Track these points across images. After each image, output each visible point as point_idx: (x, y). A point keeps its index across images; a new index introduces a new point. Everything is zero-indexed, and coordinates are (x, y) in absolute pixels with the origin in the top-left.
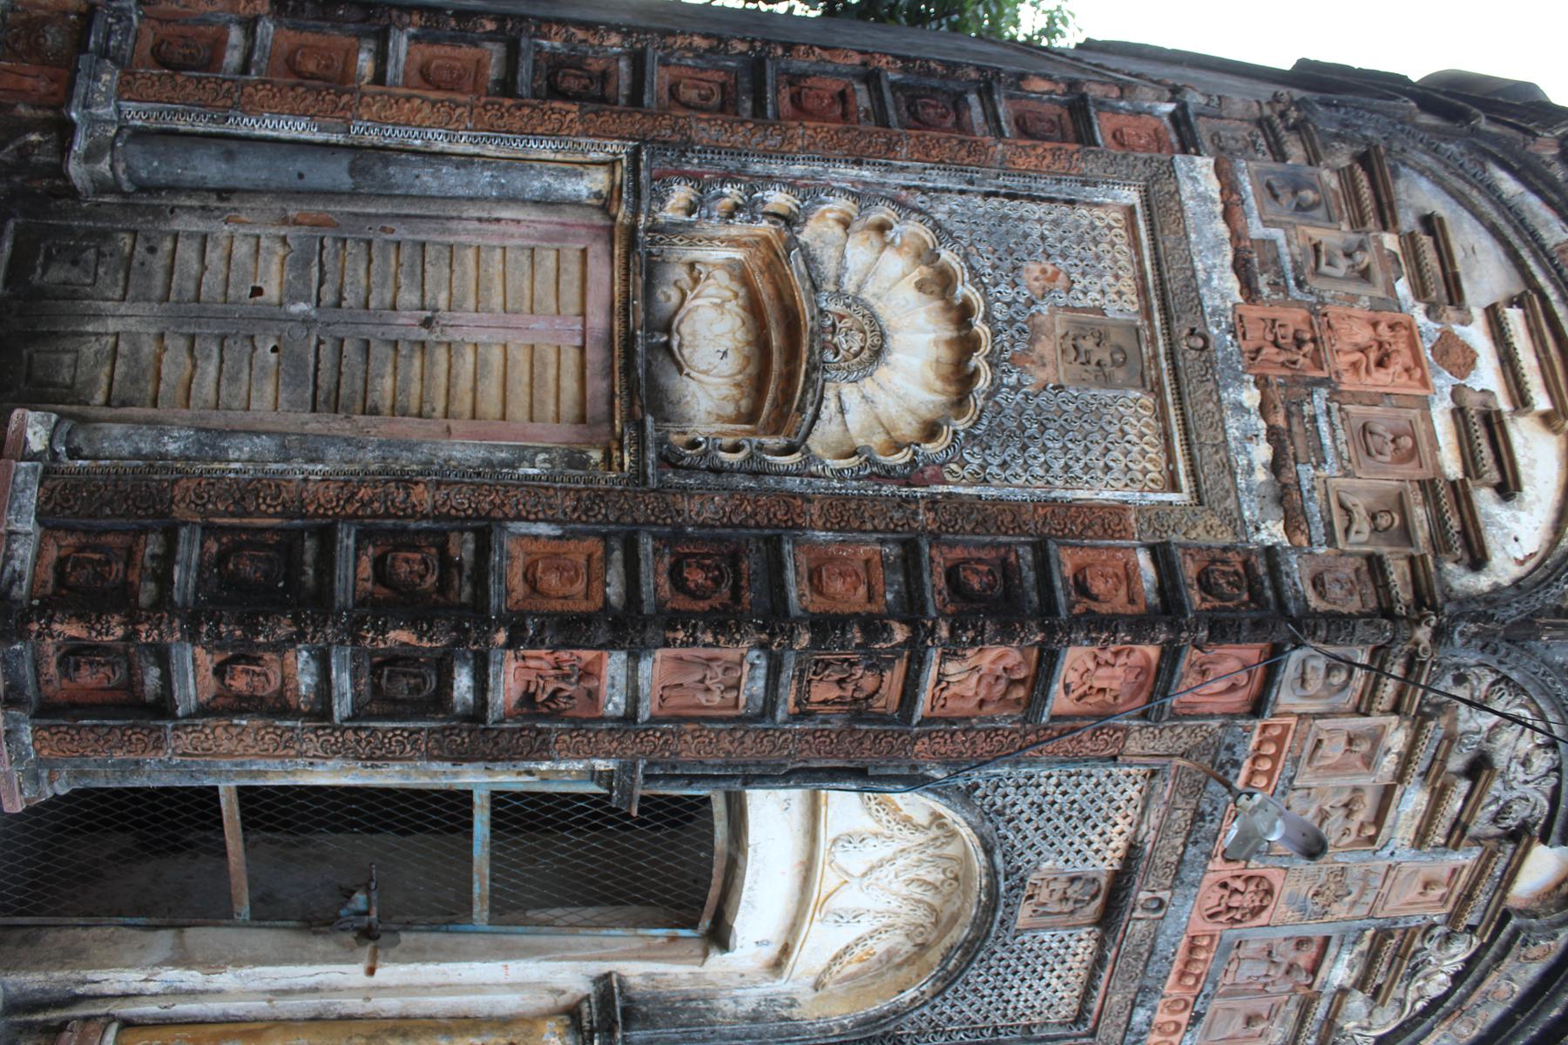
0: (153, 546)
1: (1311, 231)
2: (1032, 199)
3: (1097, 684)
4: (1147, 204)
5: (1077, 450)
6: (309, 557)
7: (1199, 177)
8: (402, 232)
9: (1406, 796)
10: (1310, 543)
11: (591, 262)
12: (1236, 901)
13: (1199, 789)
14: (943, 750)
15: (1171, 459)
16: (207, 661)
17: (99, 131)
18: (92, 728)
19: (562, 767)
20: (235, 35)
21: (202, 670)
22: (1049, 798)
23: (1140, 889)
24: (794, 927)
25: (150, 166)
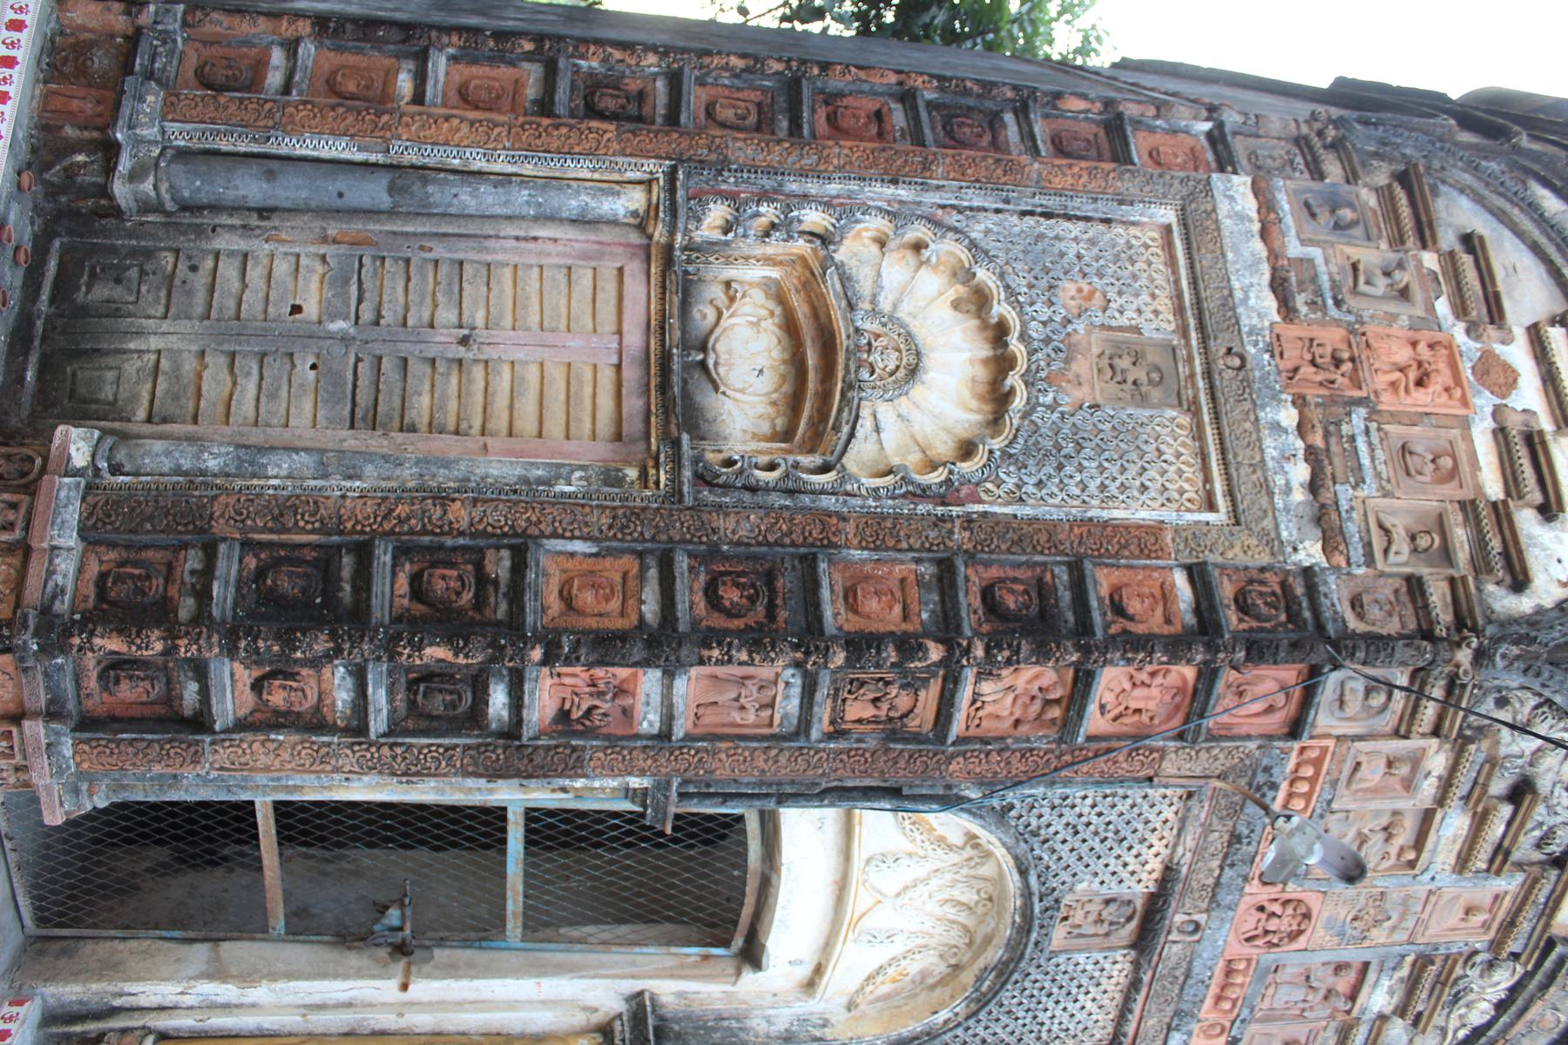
0: (193, 561)
1: (1349, 250)
2: (1068, 218)
3: (1133, 705)
4: (1184, 223)
5: (1114, 469)
6: (346, 573)
7: (1235, 196)
8: (440, 251)
9: (1447, 820)
10: (1349, 563)
11: (627, 280)
12: (1273, 925)
13: (1235, 811)
14: (978, 770)
15: (1207, 479)
16: (245, 676)
17: (143, 151)
18: (131, 742)
19: (597, 784)
20: (277, 57)
21: (240, 685)
22: (1084, 819)
23: (1176, 912)
24: (827, 947)
25: (193, 186)
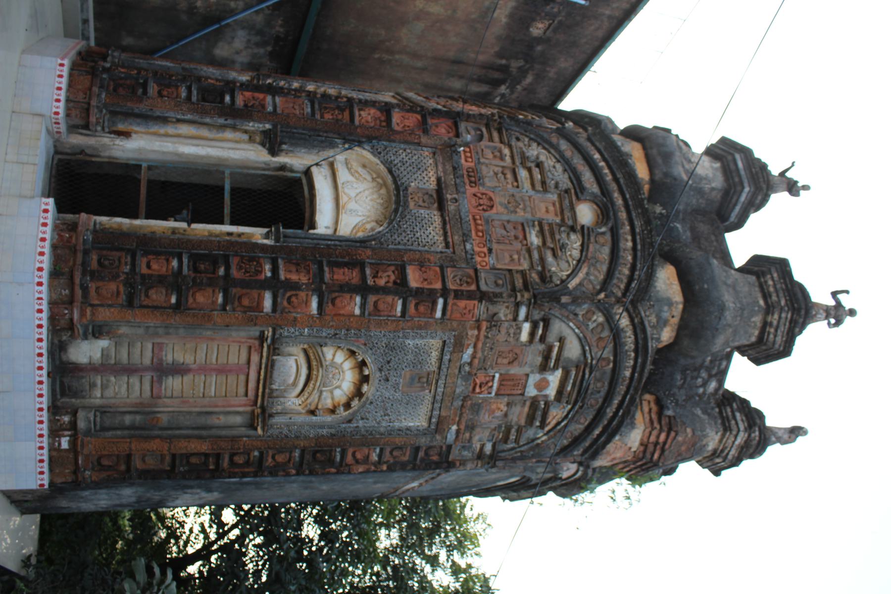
12: (481, 202)
13: (451, 158)
24: (337, 222)
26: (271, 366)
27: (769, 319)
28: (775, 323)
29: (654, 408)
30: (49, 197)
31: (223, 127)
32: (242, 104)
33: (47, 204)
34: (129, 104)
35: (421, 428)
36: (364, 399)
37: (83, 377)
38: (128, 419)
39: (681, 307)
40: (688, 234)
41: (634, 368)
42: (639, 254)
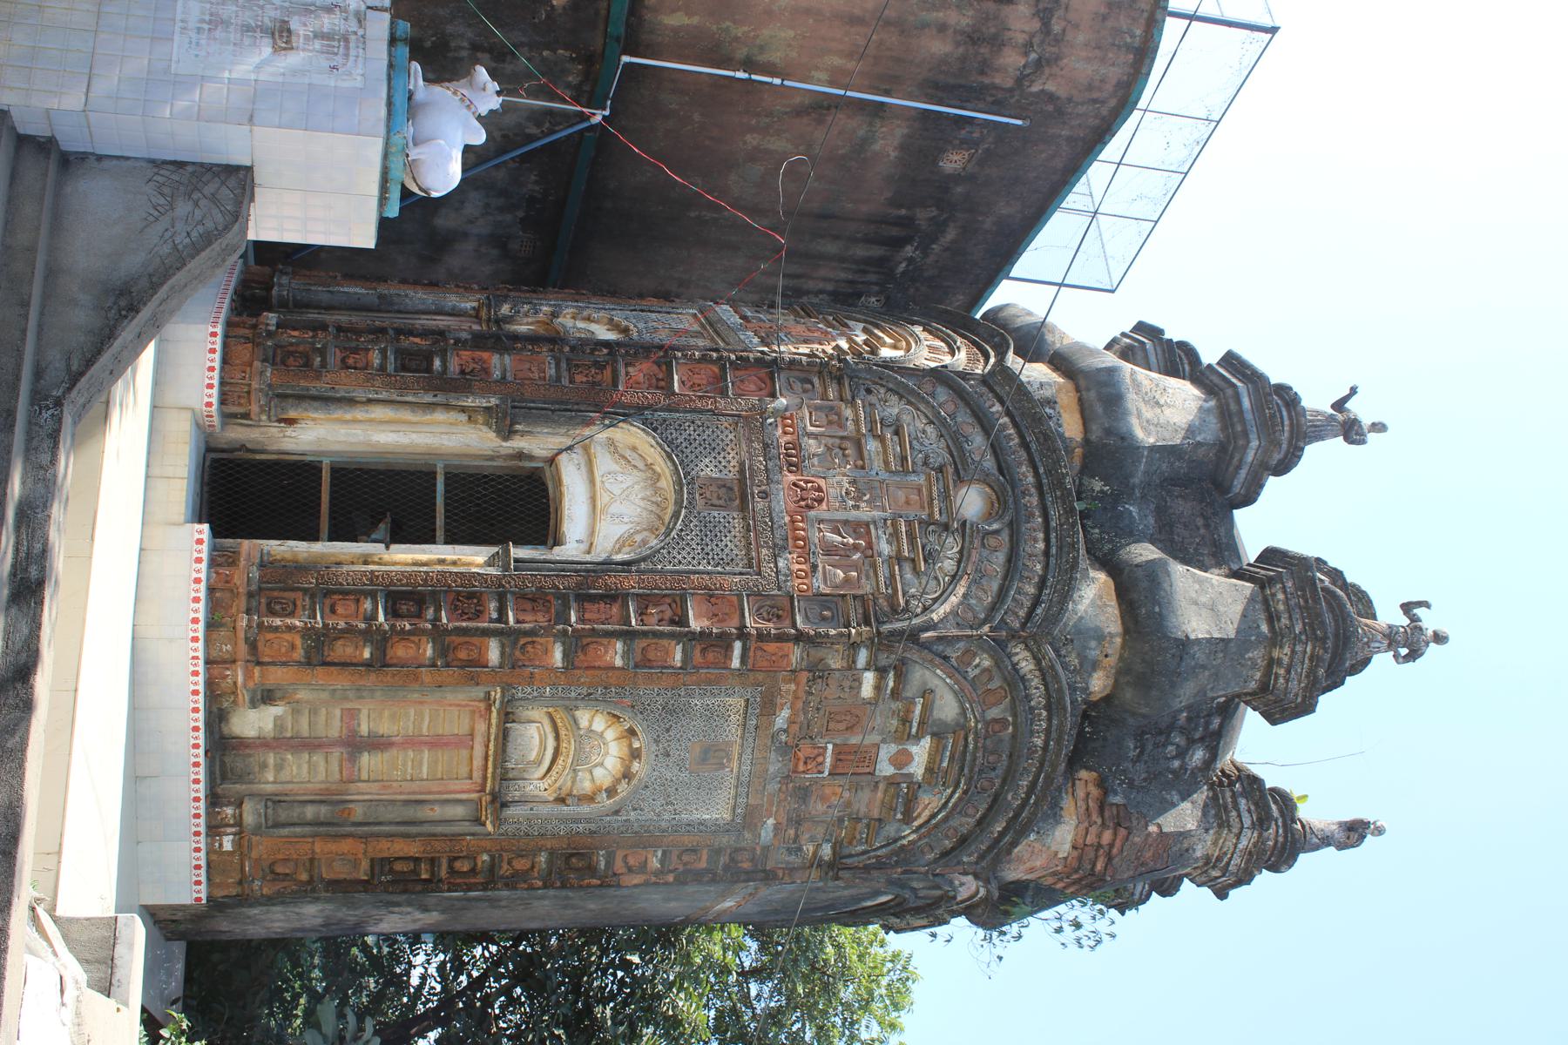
24: (592, 533)
26: (504, 735)
27: (1276, 654)
28: (1286, 660)
29: (1095, 792)
30: (200, 522)
31: (431, 406)
32: (457, 370)
33: (201, 532)
34: (303, 383)
35: (721, 822)
36: (635, 782)
37: (250, 756)
38: (310, 812)
39: (1118, 640)
40: (1151, 520)
41: (1048, 731)
42: (1052, 561)
